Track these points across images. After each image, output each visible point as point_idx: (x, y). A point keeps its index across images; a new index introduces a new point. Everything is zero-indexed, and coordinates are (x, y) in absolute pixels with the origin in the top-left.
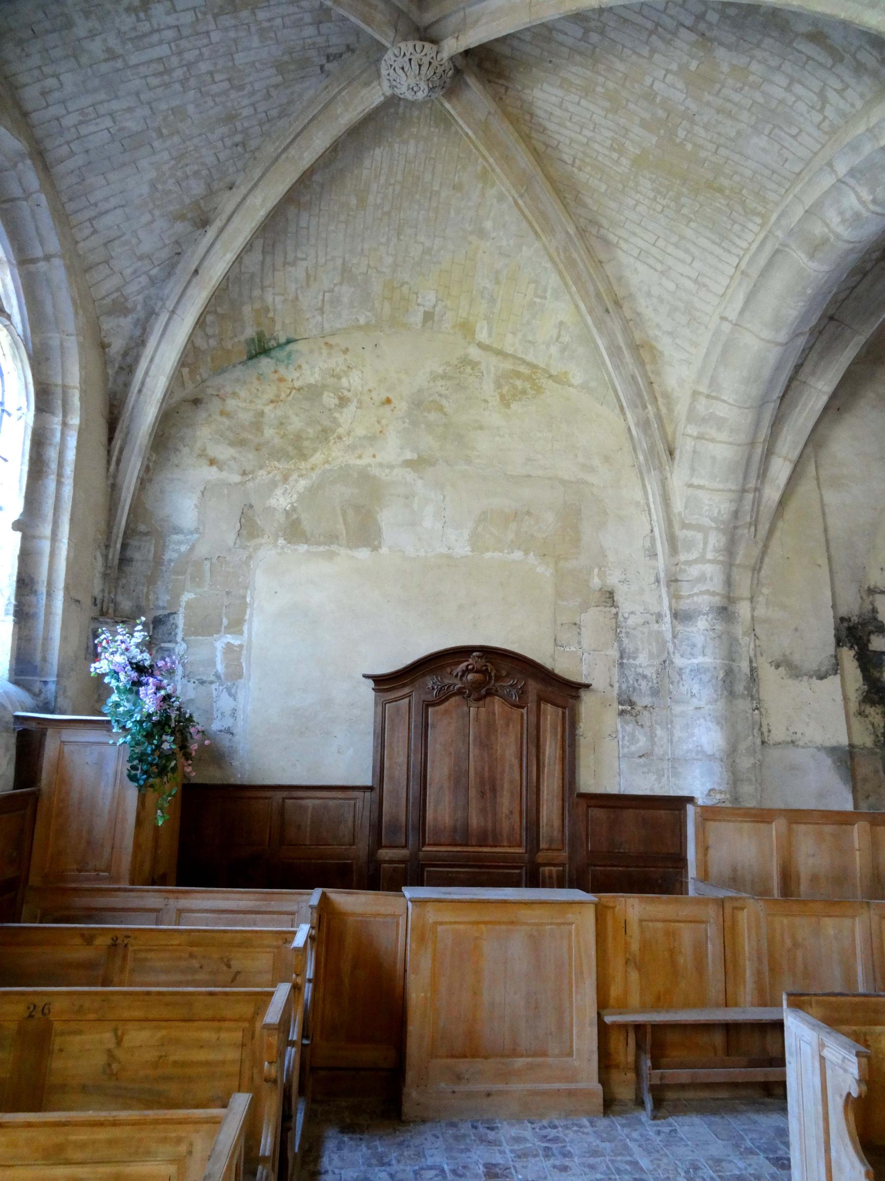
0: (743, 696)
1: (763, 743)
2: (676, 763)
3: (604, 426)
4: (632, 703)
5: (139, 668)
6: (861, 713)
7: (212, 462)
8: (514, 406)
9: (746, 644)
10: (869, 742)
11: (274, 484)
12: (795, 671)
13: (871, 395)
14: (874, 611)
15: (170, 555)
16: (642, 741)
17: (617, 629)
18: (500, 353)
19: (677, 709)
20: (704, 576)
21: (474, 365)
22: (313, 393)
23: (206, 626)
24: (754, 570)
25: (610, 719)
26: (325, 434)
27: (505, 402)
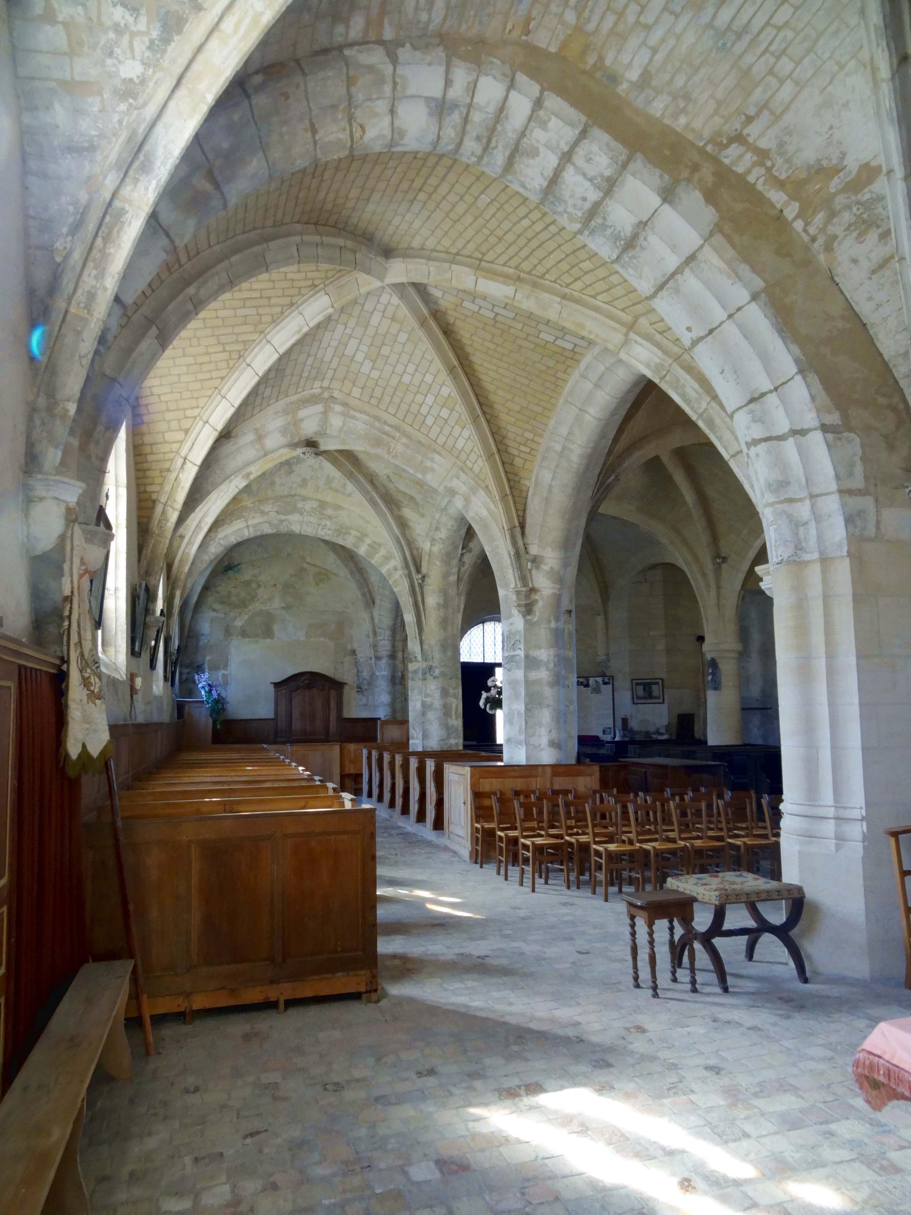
3: (352, 591)
5: (209, 685)
7: (214, 610)
8: (321, 585)
11: (236, 618)
15: (201, 643)
16: (364, 701)
17: (356, 663)
18: (314, 565)
19: (376, 690)
20: (385, 646)
21: (306, 570)
22: (248, 583)
23: (214, 668)
25: (354, 693)
26: (253, 598)
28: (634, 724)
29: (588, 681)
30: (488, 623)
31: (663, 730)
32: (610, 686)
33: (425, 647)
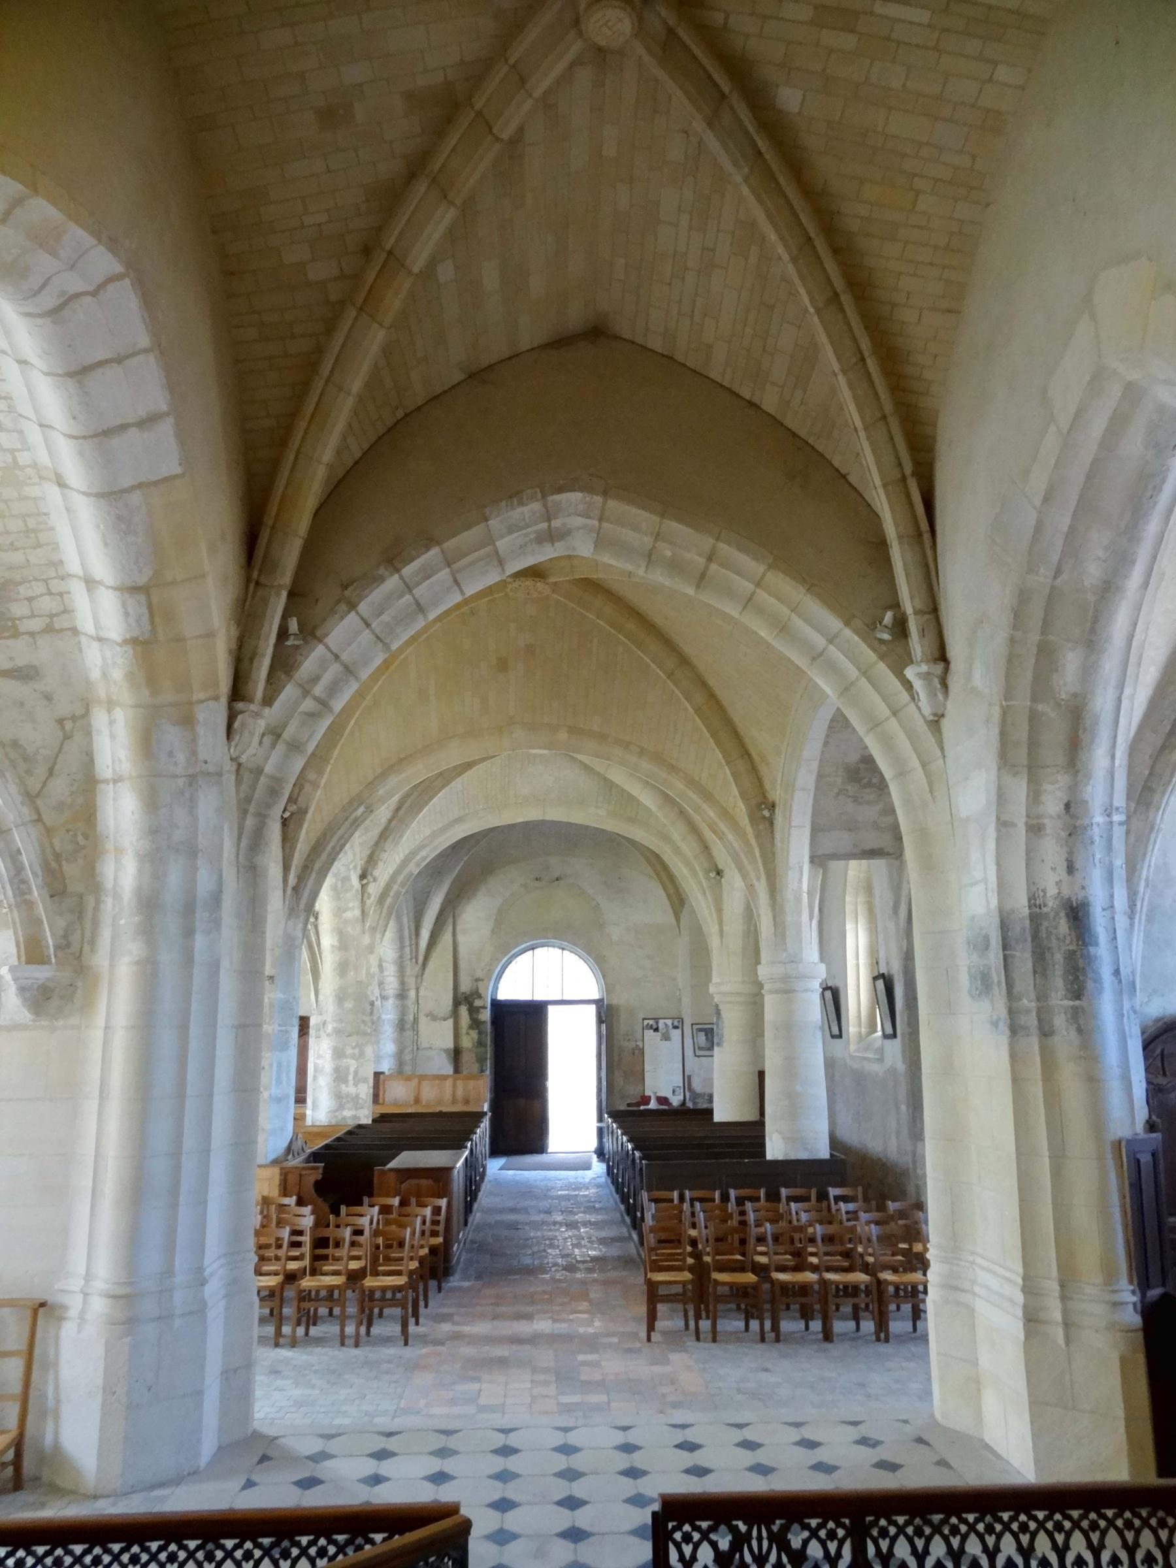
9: (412, 1007)
12: (433, 1017)
28: (697, 1085)
32: (679, 1031)
33: (321, 997)
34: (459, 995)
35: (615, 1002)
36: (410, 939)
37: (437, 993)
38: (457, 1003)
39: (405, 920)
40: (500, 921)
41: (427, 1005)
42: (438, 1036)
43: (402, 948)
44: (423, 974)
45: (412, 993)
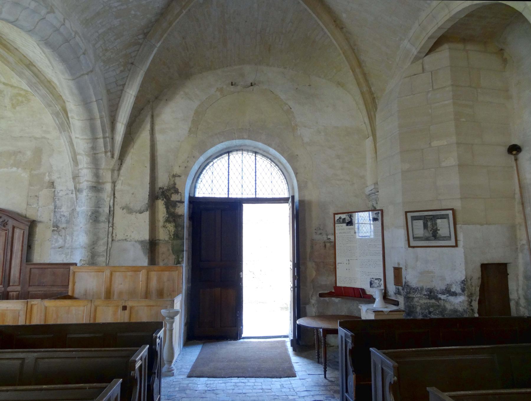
0: (104, 222)
1: (112, 240)
2: (73, 249)
4: (57, 227)
6: (164, 226)
8: (17, 108)
10: (167, 238)
12: (129, 210)
13: (182, 93)
14: (175, 184)
16: (61, 242)
17: (54, 197)
18: (12, 86)
24: (113, 171)
27: (14, 106)
28: (411, 277)
29: (351, 217)
30: (235, 153)
31: (456, 288)
34: (157, 189)
35: (307, 198)
36: (104, 132)
37: (133, 185)
38: (153, 197)
39: (95, 107)
40: (198, 118)
41: (122, 199)
42: (134, 228)
43: (94, 139)
44: (119, 169)
45: (108, 187)
